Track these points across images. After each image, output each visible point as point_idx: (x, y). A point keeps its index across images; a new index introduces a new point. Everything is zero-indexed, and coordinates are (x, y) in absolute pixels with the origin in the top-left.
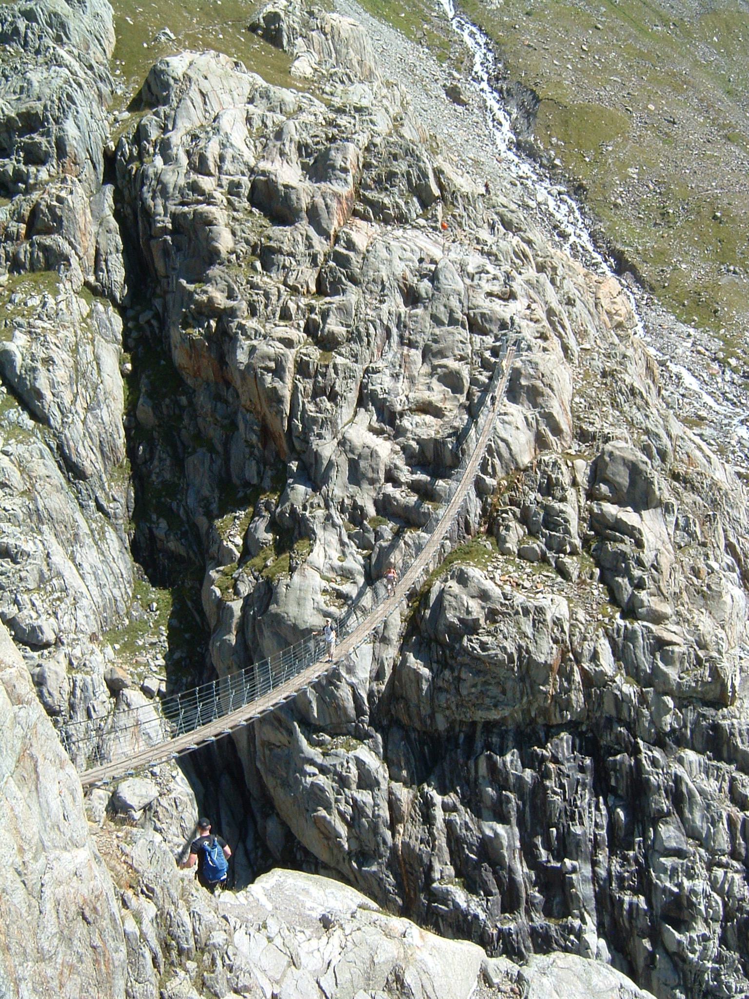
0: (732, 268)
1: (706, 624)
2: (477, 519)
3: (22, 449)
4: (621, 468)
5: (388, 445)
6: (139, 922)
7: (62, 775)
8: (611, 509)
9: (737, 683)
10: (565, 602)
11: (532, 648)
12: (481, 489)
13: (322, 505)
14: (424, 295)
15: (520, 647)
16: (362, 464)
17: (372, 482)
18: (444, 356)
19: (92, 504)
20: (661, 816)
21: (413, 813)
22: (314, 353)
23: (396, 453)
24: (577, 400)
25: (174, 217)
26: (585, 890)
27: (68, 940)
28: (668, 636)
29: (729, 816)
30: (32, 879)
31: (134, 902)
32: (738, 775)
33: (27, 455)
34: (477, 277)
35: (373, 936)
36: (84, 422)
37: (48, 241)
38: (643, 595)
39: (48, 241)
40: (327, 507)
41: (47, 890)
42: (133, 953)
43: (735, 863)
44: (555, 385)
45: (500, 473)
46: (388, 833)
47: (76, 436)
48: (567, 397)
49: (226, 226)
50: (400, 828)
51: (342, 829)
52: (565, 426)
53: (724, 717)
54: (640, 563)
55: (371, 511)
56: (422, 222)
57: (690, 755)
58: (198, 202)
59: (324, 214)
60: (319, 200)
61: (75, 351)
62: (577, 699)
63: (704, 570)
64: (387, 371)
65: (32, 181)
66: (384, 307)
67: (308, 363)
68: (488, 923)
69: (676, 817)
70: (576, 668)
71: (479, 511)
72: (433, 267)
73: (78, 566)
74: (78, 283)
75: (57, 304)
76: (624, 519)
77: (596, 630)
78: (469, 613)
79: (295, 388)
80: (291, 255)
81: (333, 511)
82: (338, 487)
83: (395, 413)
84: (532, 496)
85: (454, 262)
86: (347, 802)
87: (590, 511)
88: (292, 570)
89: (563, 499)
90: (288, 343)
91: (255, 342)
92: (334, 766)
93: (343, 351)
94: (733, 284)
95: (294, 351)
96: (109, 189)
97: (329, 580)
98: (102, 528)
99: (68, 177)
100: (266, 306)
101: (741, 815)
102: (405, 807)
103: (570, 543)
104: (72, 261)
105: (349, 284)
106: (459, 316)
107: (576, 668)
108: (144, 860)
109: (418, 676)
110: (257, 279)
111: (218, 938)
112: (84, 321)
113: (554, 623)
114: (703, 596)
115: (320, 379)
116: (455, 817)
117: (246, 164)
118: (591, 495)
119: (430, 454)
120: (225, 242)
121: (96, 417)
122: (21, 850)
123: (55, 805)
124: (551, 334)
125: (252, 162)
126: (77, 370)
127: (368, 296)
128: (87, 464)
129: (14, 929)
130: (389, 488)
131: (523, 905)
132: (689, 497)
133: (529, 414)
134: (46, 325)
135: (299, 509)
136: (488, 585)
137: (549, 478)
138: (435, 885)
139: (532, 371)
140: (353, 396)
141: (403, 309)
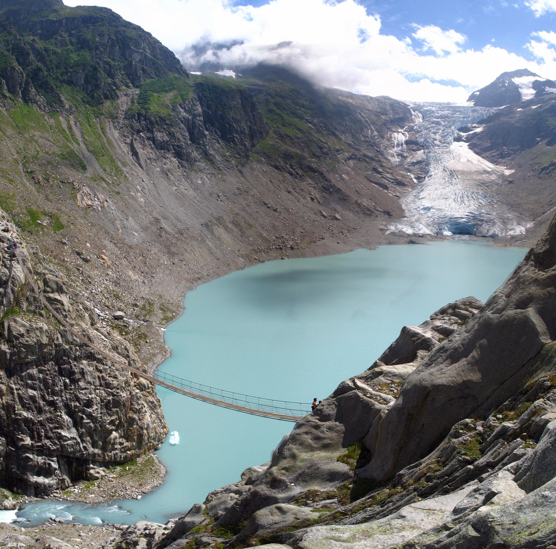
1: (84, 325)
20: (79, 380)
26: (61, 404)
54: (65, 310)
57: (85, 362)
62: (54, 352)
69: (83, 379)
109: (5, 353)
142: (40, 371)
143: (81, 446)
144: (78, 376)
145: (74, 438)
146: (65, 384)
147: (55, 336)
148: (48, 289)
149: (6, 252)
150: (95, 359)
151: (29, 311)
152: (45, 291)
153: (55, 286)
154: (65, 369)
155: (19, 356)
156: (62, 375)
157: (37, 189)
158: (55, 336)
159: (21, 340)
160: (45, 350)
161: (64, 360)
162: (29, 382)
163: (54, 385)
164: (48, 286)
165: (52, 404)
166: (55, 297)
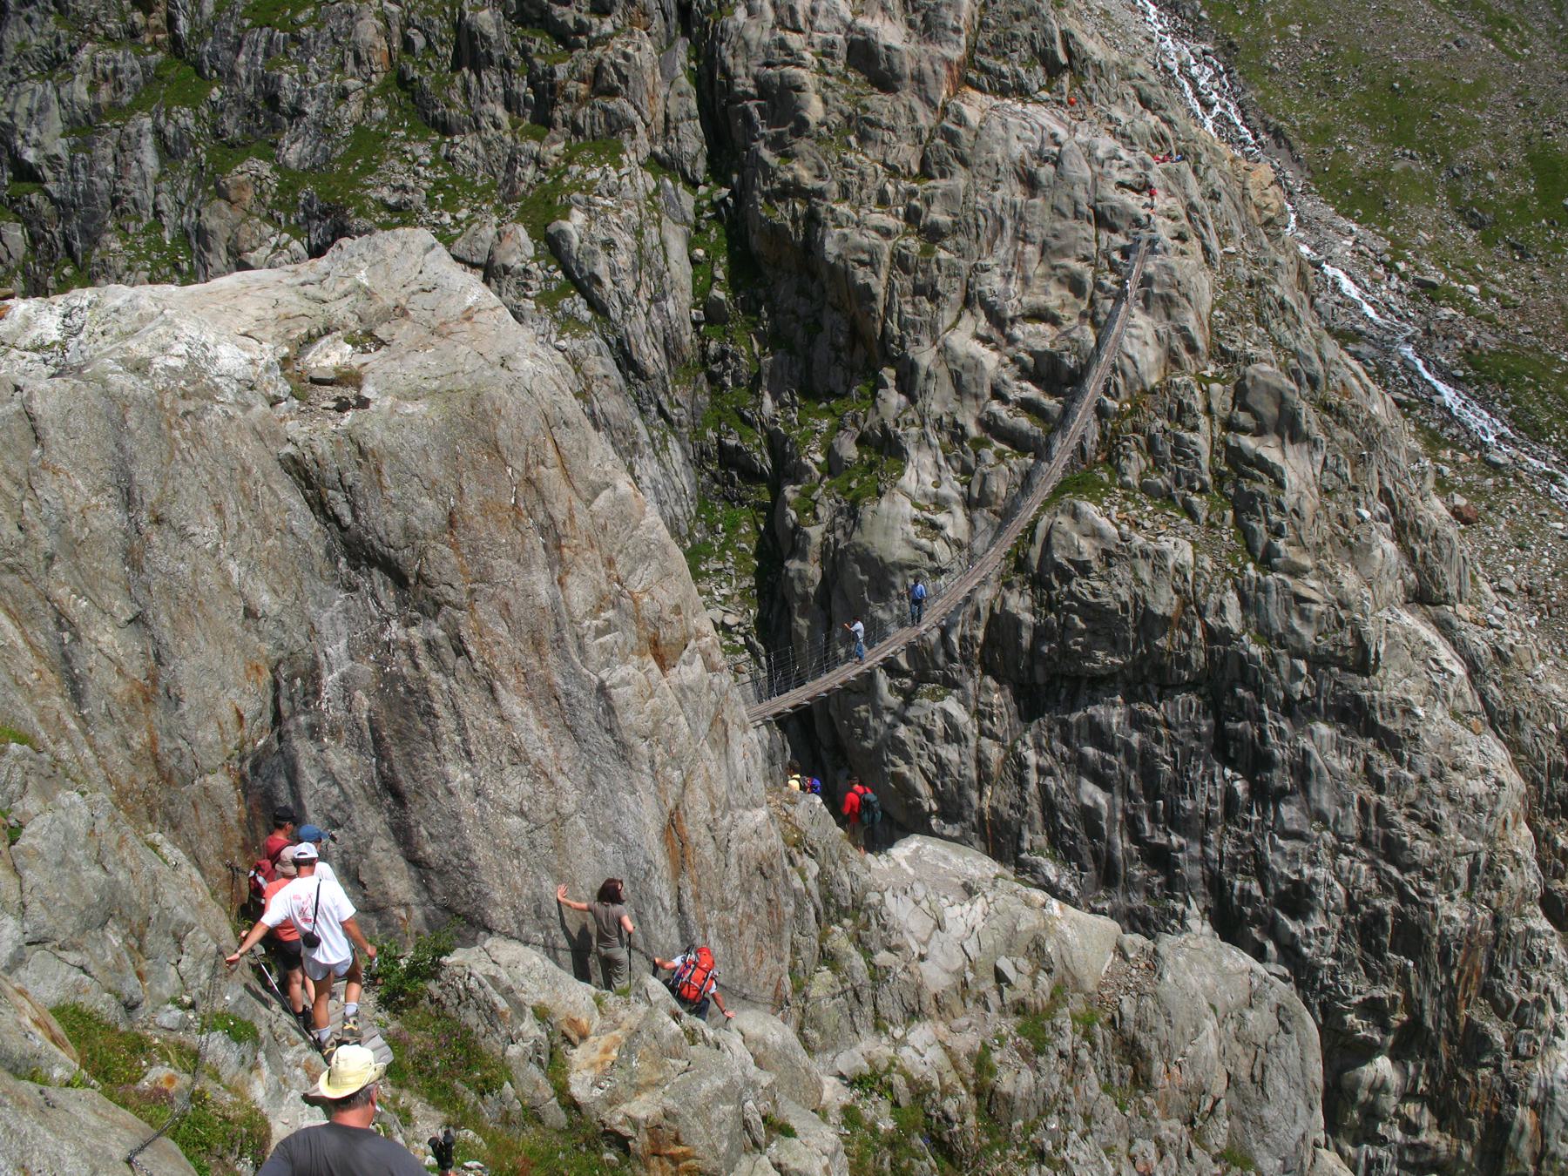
1: (1350, 580)
2: (1094, 447)
3: (577, 344)
5: (995, 355)
6: (804, 879)
7: (745, 739)
8: (1248, 442)
9: (1382, 649)
10: (1189, 548)
11: (1149, 598)
12: (1101, 411)
13: (917, 421)
14: (1044, 182)
15: (1135, 597)
16: (965, 377)
17: (976, 397)
18: (1066, 256)
19: (654, 409)
20: (1281, 795)
22: (914, 244)
23: (1005, 366)
24: (1217, 313)
25: (756, 78)
26: (1193, 872)
27: (748, 893)
28: (1305, 592)
29: (1361, 801)
30: (721, 835)
31: (799, 861)
32: (1375, 754)
33: (582, 351)
34: (1107, 163)
35: (1017, 907)
36: (647, 314)
37: (612, 105)
39: (612, 105)
40: (923, 424)
41: (733, 846)
42: (799, 906)
43: (1364, 853)
44: (1192, 295)
45: (1123, 396)
46: (974, 795)
47: (638, 331)
48: (1205, 309)
49: (817, 92)
50: (988, 791)
51: (923, 788)
52: (1201, 344)
53: (1364, 688)
54: (1280, 507)
55: (973, 431)
56: (1044, 94)
57: (1323, 729)
58: (786, 64)
59: (931, 82)
60: (926, 65)
61: (638, 233)
62: (1198, 657)
64: (998, 270)
65: (594, 34)
66: (998, 194)
67: (907, 257)
69: (1299, 797)
70: (1198, 623)
71: (1097, 437)
72: (1056, 149)
73: (637, 479)
74: (643, 153)
75: (620, 178)
76: (1265, 455)
77: (1224, 580)
78: (1080, 553)
79: (890, 287)
80: (892, 129)
81: (928, 429)
82: (938, 401)
84: (1159, 423)
85: (1080, 145)
86: (930, 759)
87: (1225, 443)
88: (880, 494)
89: (1195, 429)
90: (886, 233)
91: (846, 231)
93: (948, 243)
94: (1407, 171)
95: (891, 242)
96: (682, 45)
97: (921, 508)
98: (664, 436)
99: (636, 29)
100: (861, 188)
101: (1375, 798)
103: (1201, 480)
104: (638, 128)
105: (958, 166)
106: (1084, 208)
107: (1198, 623)
108: (806, 821)
109: (1018, 623)
110: (850, 157)
111: (873, 898)
112: (650, 198)
113: (1177, 570)
115: (920, 275)
116: (1050, 782)
117: (842, 20)
118: (1230, 425)
119: (1044, 369)
120: (814, 110)
121: (660, 309)
122: (713, 808)
123: (740, 766)
124: (1191, 234)
125: (849, 17)
126: (641, 256)
127: (979, 181)
128: (649, 362)
129: (704, 879)
130: (995, 406)
131: (1122, 884)
132: (1342, 434)
134: (608, 202)
135: (890, 425)
136: (1104, 523)
137: (1180, 403)
138: (1023, 856)
139: (1166, 278)
140: (956, 297)
141: (1019, 198)
142: (1137, 721)
144: (1280, 778)
146: (1230, 795)
147: (1213, 598)
148: (1243, 418)
149: (1113, 268)
150: (1370, 729)
151: (1146, 488)
153: (1270, 410)
154: (1238, 737)
155: (1063, 644)
156: (1227, 762)
158: (1213, 598)
160: (1161, 642)
161: (1241, 700)
162: (1090, 751)
163: (1181, 786)
164: (1245, 408)
165: (1160, 858)
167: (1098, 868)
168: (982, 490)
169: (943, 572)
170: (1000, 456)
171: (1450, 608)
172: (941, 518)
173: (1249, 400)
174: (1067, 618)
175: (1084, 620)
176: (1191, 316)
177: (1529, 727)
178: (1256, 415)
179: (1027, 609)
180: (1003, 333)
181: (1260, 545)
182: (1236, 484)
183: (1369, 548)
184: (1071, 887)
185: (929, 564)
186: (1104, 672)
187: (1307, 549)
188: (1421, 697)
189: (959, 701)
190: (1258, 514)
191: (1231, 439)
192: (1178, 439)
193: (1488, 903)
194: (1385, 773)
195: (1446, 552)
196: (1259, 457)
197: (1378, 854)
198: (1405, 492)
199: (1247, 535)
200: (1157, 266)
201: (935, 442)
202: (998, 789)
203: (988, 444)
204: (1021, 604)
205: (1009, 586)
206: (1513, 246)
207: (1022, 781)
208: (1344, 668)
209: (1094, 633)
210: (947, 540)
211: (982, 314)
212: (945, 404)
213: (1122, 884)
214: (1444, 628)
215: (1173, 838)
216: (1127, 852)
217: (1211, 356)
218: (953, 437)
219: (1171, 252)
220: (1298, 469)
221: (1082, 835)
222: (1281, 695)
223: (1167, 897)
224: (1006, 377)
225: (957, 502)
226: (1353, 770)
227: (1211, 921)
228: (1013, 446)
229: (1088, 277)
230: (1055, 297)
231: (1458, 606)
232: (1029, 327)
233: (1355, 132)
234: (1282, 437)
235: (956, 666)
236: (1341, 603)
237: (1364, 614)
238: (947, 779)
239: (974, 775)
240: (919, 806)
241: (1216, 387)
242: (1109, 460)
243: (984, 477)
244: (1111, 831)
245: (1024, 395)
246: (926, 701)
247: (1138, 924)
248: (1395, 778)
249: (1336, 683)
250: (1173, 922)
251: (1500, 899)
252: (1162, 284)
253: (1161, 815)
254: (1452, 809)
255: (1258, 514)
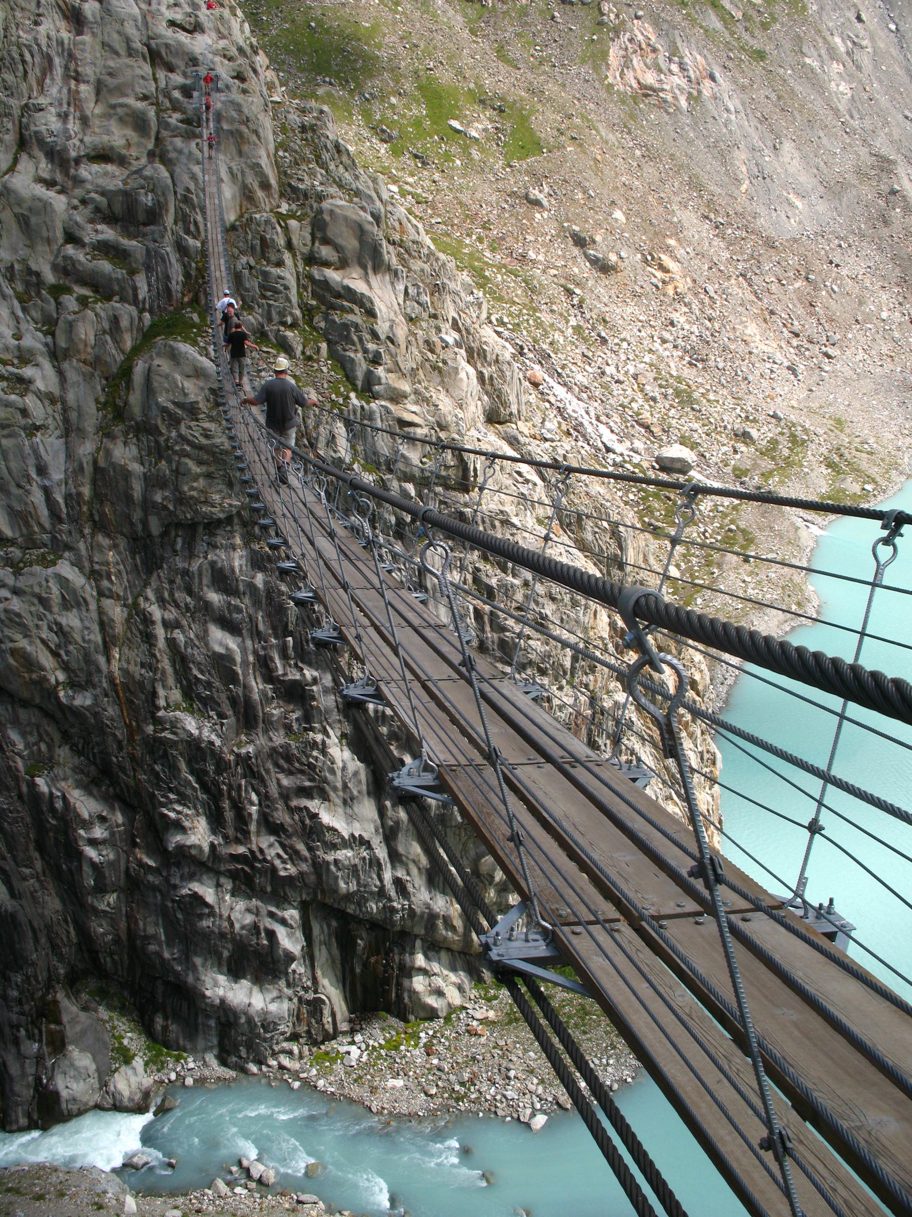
0: (327, 79)
1: (445, 404)
2: (179, 288)
4: (344, 229)
5: (63, 198)
9: (478, 466)
16: (33, 220)
17: (49, 241)
21: (129, 635)
23: (75, 208)
24: (281, 153)
26: (327, 702)
28: (408, 417)
29: (476, 609)
32: (481, 565)
38: (380, 371)
44: (260, 130)
46: (102, 660)
48: (272, 147)
51: (46, 660)
52: (273, 182)
54: (375, 335)
55: (50, 277)
63: (439, 344)
68: (225, 749)
71: (181, 278)
78: (186, 395)
83: (68, 161)
84: (244, 260)
86: (50, 629)
87: (310, 277)
89: (280, 264)
92: (32, 586)
101: (487, 608)
102: (119, 629)
103: (291, 314)
106: (138, 45)
109: (126, 475)
114: (440, 372)
118: (311, 260)
119: (118, 208)
130: (70, 250)
131: (261, 725)
133: (233, 164)
137: (263, 240)
138: (161, 713)
139: (234, 114)
143: (388, 876)
145: (363, 842)
148: (325, 252)
152: (311, 260)
153: (351, 243)
155: (177, 489)
157: (470, 21)
159: (191, 429)
162: (214, 597)
164: (326, 241)
165: (296, 694)
166: (346, 282)
167: (236, 713)
168: (70, 340)
169: (38, 428)
170: (83, 302)
171: (514, 426)
172: (28, 372)
173: (330, 234)
174: (179, 463)
175: (200, 463)
176: (263, 153)
177: (589, 524)
178: (337, 248)
179: (135, 459)
180: (67, 174)
181: (360, 374)
182: (326, 318)
183: (456, 370)
184: (213, 737)
185: (23, 422)
186: (222, 516)
187: (404, 375)
188: (513, 507)
189: (73, 564)
190: (354, 344)
191: (316, 272)
192: (265, 274)
193: (587, 686)
194: (493, 582)
195: (508, 374)
196: (348, 289)
197: (495, 657)
198: (468, 321)
199: (344, 365)
200: (223, 103)
201: (9, 291)
202: (126, 650)
203: (68, 290)
204: (128, 454)
205: (110, 436)
206: (416, 156)
207: (149, 638)
208: (447, 487)
209: (209, 476)
210: (39, 395)
211: (41, 156)
212: (14, 250)
213: (261, 725)
214: (513, 441)
215: (305, 672)
216: (263, 693)
217: (282, 195)
218: (27, 284)
219: (234, 90)
220: (385, 297)
221: (217, 684)
222: (393, 519)
223: (306, 729)
224: (78, 219)
225: (42, 354)
226: (465, 583)
227: (348, 745)
228: (96, 291)
229: (152, 113)
230: (117, 136)
231: (519, 423)
232: (95, 168)
233: (283, 62)
234: (364, 267)
235: (65, 527)
236: (439, 425)
237: (459, 433)
238: (71, 648)
239: (99, 639)
240: (45, 679)
241: (293, 223)
242: (195, 301)
243: (71, 326)
244: (245, 675)
245: (100, 237)
246: (37, 568)
247: (282, 762)
248: (503, 586)
249: (441, 502)
250: (315, 753)
251: (596, 681)
252: (232, 121)
253: (291, 652)
254: (554, 607)
255: (354, 344)
